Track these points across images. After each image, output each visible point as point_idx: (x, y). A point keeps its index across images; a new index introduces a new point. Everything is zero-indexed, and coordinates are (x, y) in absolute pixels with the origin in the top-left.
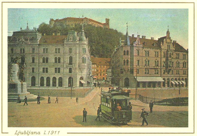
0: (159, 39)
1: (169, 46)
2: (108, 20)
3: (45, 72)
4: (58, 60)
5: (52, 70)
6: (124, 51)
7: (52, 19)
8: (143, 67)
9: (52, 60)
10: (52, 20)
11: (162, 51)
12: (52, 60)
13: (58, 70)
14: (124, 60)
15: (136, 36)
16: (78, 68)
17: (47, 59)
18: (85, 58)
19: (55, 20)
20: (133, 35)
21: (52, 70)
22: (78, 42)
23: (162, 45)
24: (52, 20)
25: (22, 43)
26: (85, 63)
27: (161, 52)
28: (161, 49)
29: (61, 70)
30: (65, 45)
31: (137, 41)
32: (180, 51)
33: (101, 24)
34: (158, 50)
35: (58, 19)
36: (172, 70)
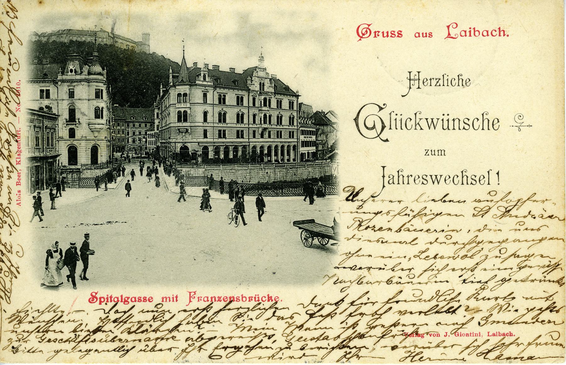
0: (245, 71)
1: (262, 85)
6: (179, 95)
8: (216, 125)
11: (251, 94)
14: (179, 112)
15: (200, 65)
20: (195, 64)
23: (249, 82)
27: (249, 95)
28: (248, 90)
30: (59, 83)
31: (202, 75)
32: (284, 95)
34: (244, 93)
36: (270, 130)
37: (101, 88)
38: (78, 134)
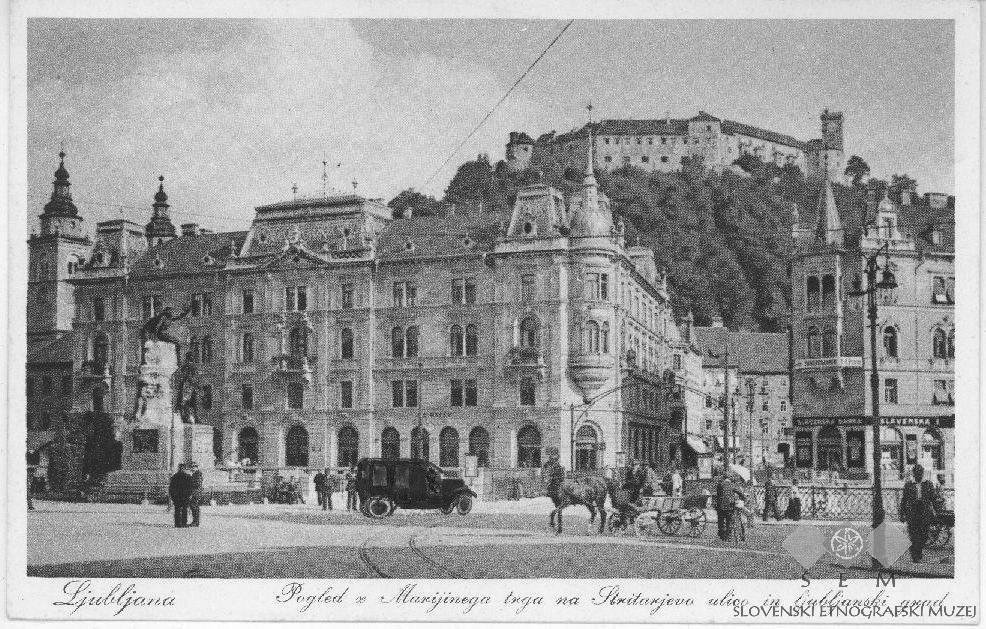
2: (831, 120)
3: (405, 403)
4: (465, 340)
5: (433, 394)
7: (523, 135)
9: (433, 341)
10: (518, 139)
12: (433, 341)
13: (463, 395)
16: (565, 383)
17: (413, 333)
18: (601, 324)
19: (535, 135)
21: (433, 394)
22: (563, 243)
24: (518, 139)
25: (296, 260)
26: (606, 350)
29: (483, 395)
30: (499, 262)
33: (791, 142)
35: (550, 135)
37: (603, 271)
38: (541, 396)
